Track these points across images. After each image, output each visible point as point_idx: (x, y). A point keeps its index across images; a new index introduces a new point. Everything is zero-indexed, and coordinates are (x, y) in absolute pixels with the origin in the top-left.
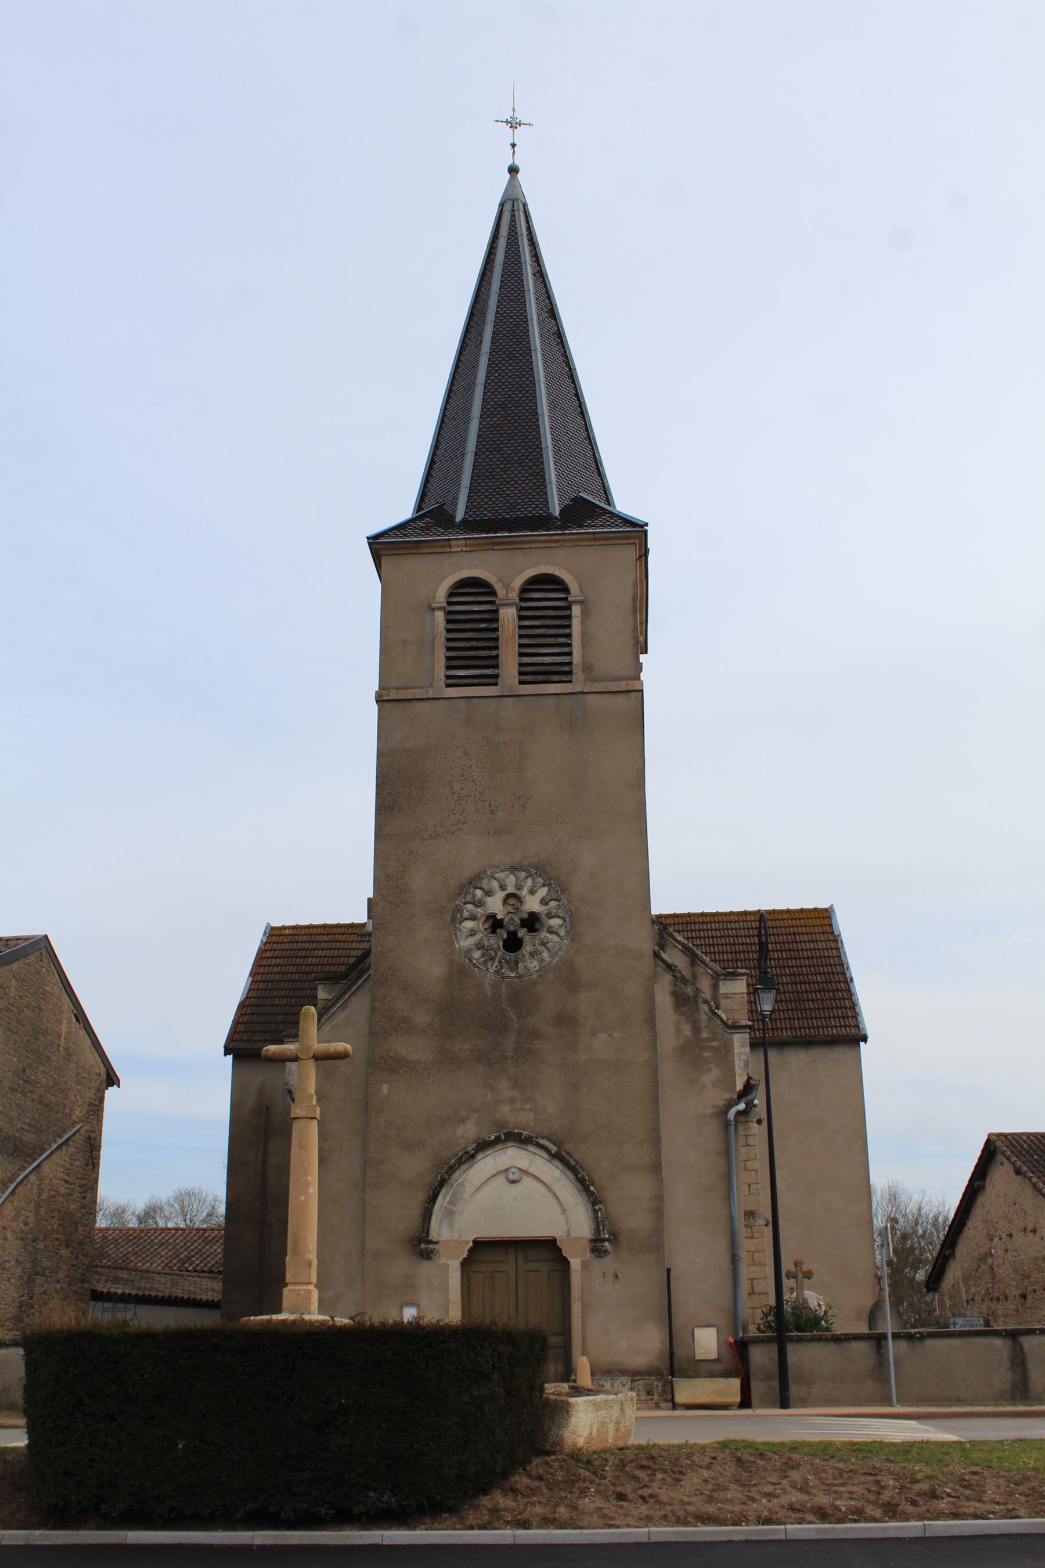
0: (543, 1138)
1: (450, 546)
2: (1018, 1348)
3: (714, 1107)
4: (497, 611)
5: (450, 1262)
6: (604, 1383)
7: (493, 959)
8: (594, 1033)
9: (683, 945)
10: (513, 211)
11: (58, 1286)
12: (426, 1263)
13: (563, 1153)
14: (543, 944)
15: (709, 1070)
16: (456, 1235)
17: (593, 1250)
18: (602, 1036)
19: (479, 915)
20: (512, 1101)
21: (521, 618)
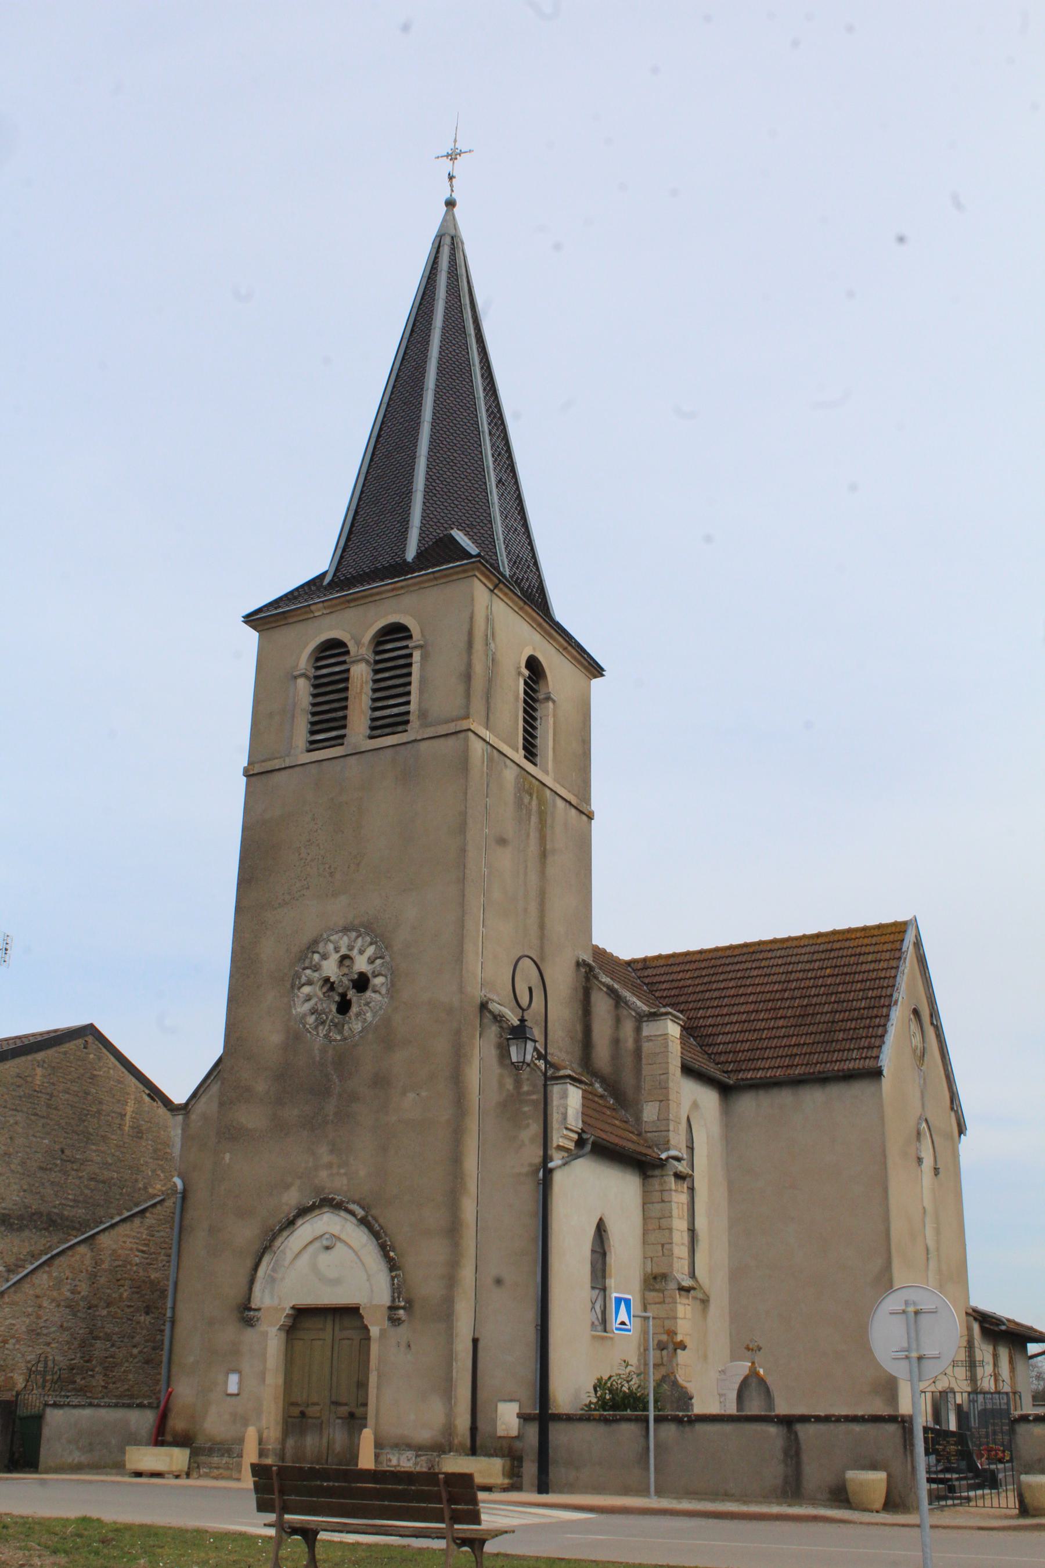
0: (354, 1202)
1: (312, 612)
2: (793, 1437)
3: (530, 1165)
4: (348, 670)
7: (323, 1023)
8: (404, 1093)
9: (608, 987)
10: (453, 244)
11: (135, 1351)
12: (250, 1329)
13: (370, 1218)
14: (367, 1004)
15: (528, 1125)
17: (390, 1319)
18: (411, 1096)
19: (315, 979)
20: (329, 1166)
21: (376, 672)
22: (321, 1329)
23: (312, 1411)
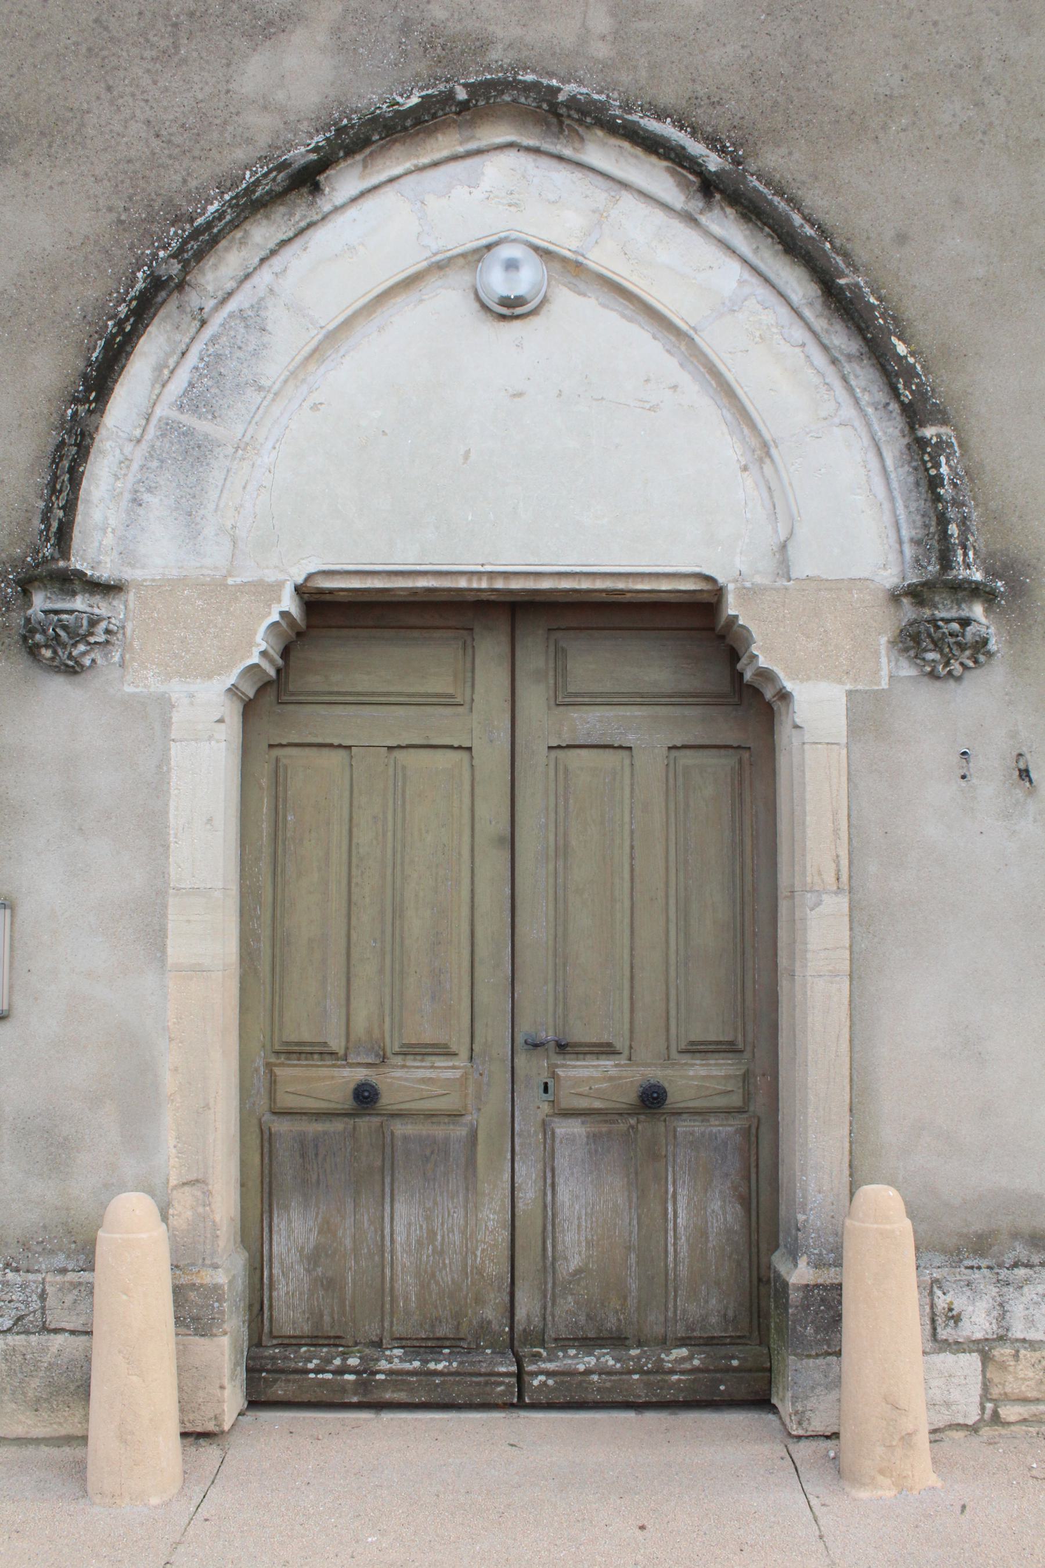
5: (176, 689)
6: (960, 1303)
12: (57, 688)
16: (214, 557)
17: (913, 641)
22: (446, 701)
23: (404, 1082)
